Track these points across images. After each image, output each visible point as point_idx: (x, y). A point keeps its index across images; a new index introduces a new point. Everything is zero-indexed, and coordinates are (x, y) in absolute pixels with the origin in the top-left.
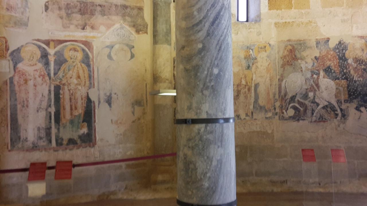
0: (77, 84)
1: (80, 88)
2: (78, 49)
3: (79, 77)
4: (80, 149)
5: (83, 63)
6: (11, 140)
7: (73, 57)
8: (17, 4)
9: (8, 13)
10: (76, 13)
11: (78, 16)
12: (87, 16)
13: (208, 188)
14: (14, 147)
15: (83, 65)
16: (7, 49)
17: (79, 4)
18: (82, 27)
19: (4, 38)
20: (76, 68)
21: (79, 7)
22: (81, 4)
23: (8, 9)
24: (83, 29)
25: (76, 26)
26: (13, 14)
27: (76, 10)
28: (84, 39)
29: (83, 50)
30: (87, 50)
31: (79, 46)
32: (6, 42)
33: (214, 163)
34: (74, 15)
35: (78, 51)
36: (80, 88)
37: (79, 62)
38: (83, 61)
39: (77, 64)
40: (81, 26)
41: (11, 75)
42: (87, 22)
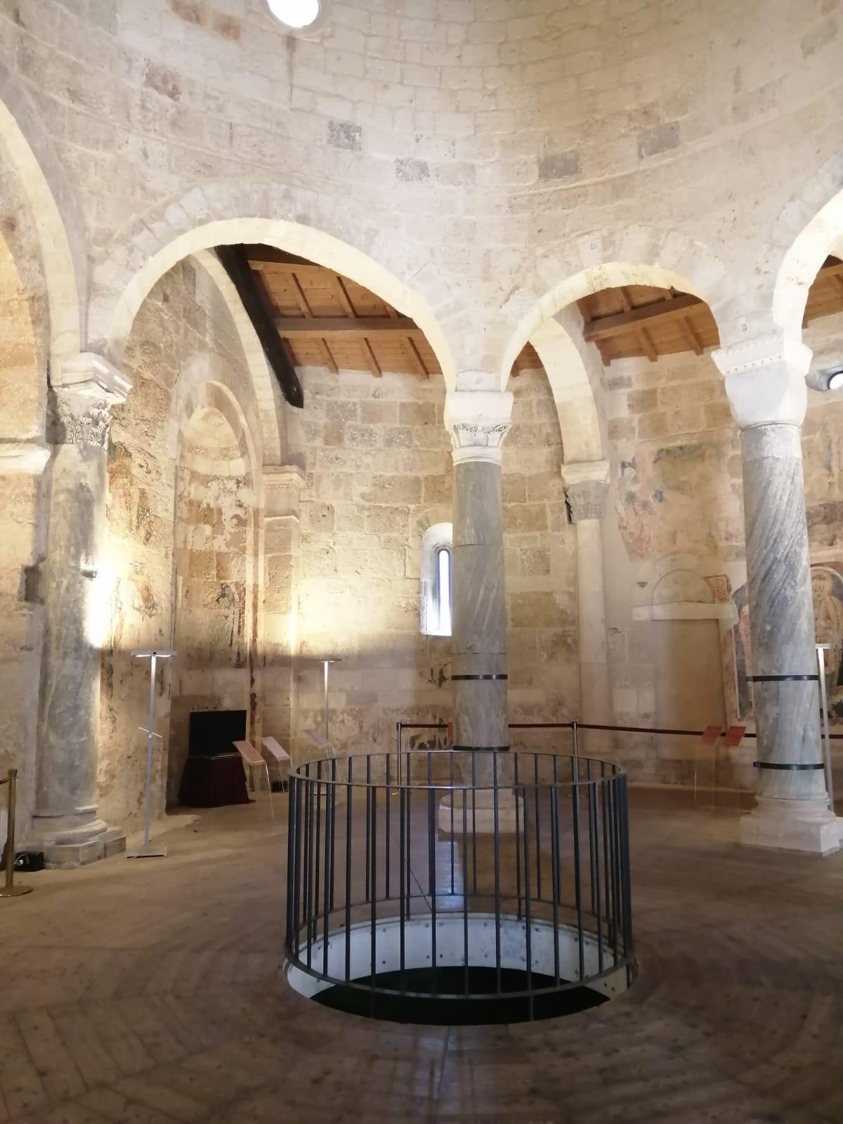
0: (826, 628)
1: (831, 633)
2: (825, 575)
3: (828, 617)
4: (836, 726)
5: (834, 595)
6: (740, 706)
7: (818, 589)
8: (738, 530)
9: (729, 544)
10: (820, 523)
11: (823, 527)
12: (836, 524)
13: (767, 746)
14: (745, 715)
15: (834, 598)
16: (729, 590)
17: (822, 509)
18: (830, 542)
19: (725, 576)
20: (823, 604)
21: (822, 514)
22: (826, 508)
23: (727, 539)
24: (831, 544)
25: (821, 542)
26: (734, 543)
27: (819, 519)
28: (833, 560)
29: (833, 576)
30: (838, 575)
31: (828, 572)
32: (727, 582)
33: (771, 721)
34: (817, 527)
35: (824, 579)
36: (831, 633)
37: (829, 595)
38: (833, 593)
39: (824, 599)
40: (827, 540)
41: (736, 623)
42: (837, 532)
